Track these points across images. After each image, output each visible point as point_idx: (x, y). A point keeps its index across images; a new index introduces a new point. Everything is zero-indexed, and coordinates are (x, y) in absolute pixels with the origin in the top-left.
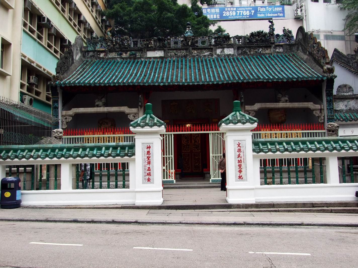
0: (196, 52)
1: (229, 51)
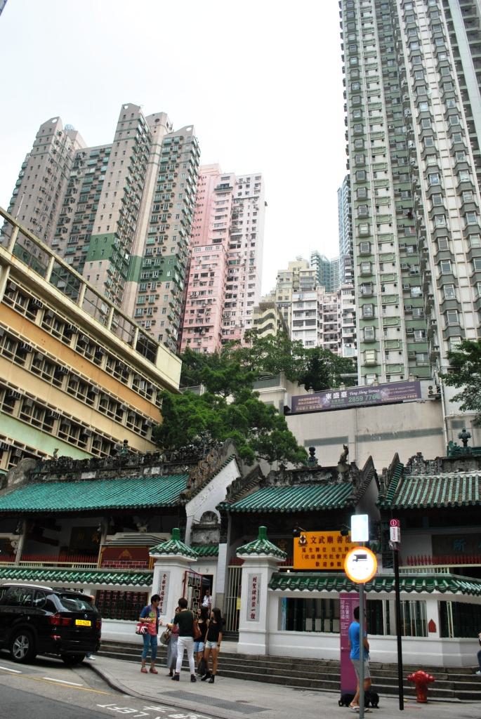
0: (125, 472)
1: (156, 471)
